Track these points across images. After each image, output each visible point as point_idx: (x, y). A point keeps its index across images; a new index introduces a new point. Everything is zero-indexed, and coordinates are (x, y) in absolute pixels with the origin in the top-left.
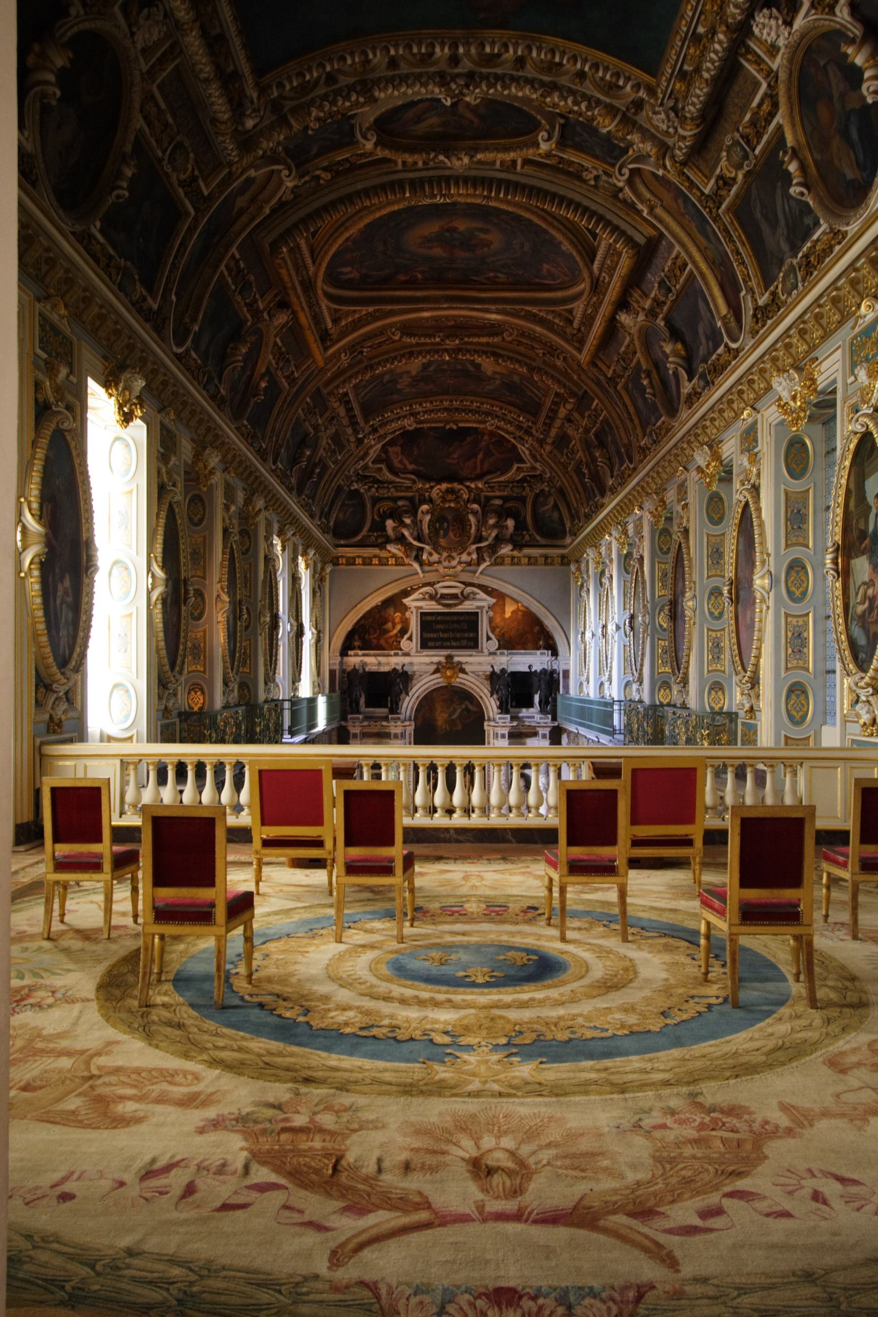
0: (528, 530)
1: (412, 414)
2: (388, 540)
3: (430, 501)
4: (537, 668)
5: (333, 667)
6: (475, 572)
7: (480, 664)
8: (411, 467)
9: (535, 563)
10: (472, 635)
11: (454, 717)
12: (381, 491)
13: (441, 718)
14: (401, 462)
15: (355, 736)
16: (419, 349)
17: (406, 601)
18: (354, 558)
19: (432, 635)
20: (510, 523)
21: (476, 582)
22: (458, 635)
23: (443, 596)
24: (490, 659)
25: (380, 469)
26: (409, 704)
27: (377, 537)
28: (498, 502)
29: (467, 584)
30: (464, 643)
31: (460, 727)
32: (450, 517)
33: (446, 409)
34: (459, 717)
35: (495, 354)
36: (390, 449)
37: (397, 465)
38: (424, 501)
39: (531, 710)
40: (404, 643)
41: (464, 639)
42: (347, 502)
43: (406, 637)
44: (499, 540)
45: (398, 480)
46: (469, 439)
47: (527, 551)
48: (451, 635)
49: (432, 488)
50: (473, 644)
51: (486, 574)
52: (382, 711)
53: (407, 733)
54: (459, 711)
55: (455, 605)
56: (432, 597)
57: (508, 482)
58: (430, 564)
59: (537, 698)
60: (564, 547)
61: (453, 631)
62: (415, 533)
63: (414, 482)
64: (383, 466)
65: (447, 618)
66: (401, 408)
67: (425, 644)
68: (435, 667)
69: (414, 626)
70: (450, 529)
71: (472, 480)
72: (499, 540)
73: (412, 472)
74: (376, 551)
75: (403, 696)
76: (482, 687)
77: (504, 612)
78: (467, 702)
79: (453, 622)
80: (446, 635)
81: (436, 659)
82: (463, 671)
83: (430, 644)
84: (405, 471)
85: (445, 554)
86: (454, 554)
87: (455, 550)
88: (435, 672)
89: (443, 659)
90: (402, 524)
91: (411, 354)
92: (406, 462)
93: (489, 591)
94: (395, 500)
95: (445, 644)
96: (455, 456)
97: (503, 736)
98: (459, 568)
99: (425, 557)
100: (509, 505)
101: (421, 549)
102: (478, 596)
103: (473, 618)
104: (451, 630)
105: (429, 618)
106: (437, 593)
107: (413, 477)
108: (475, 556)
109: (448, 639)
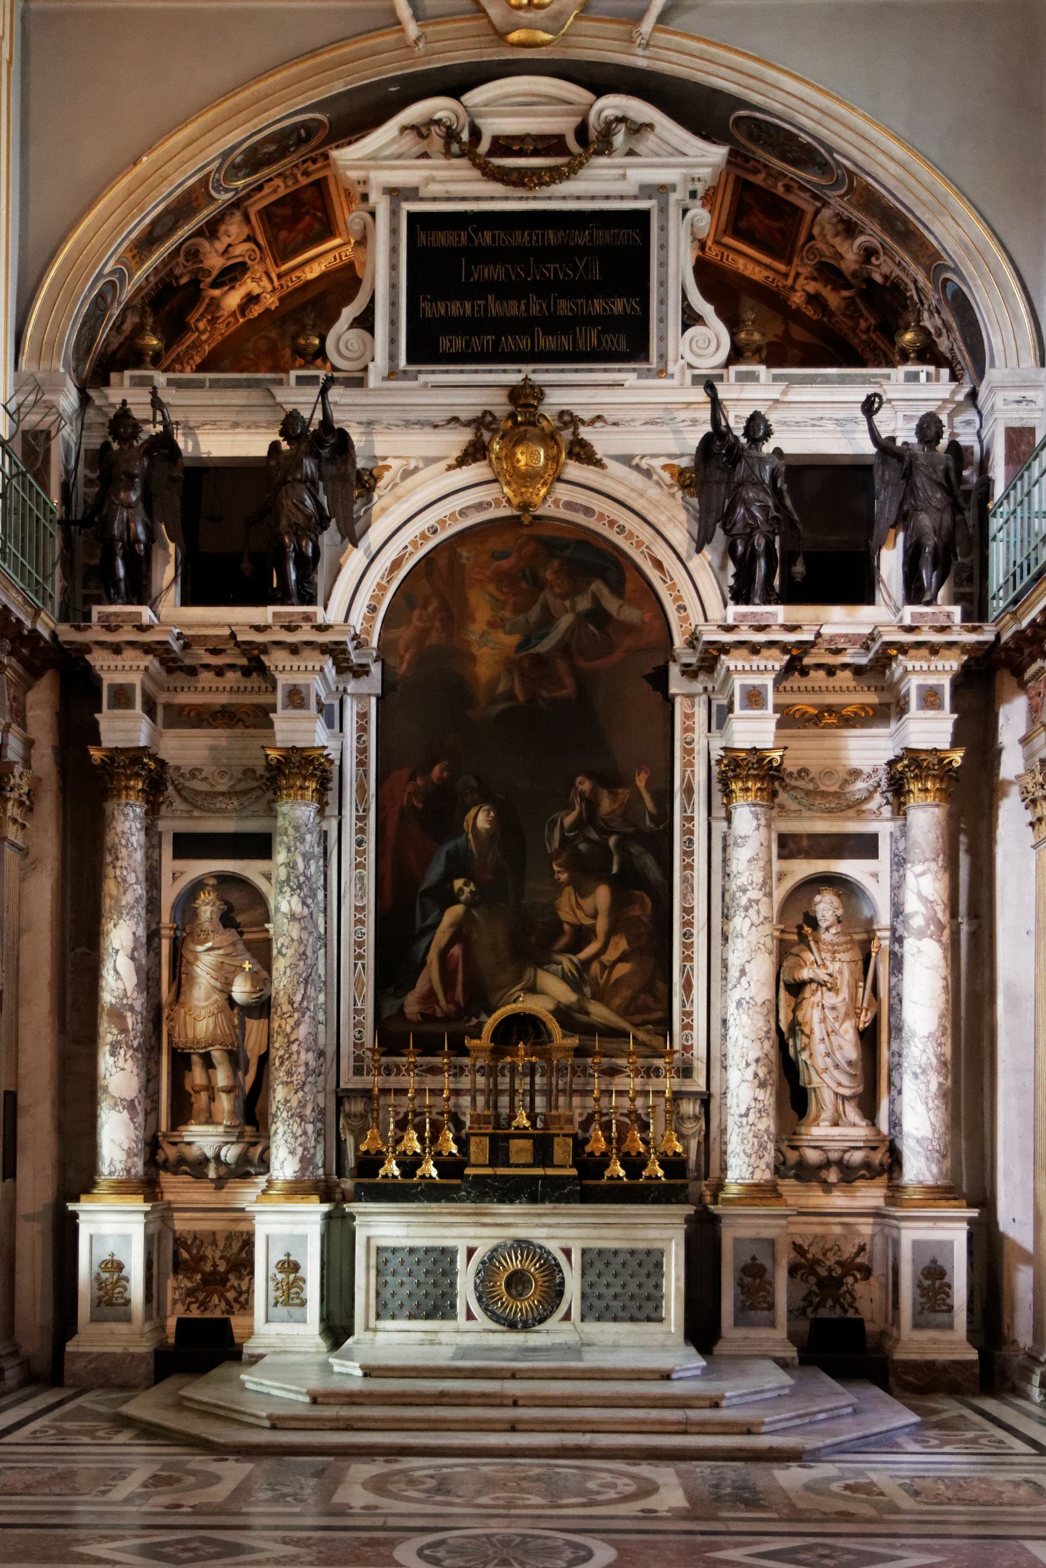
4: (899, 426)
10: (619, 306)
11: (544, 646)
13: (489, 646)
17: (350, 157)
19: (455, 309)
22: (564, 307)
23: (504, 145)
29: (600, 79)
39: (864, 612)
40: (341, 338)
43: (349, 313)
54: (565, 621)
55: (556, 175)
56: (461, 143)
59: (891, 562)
61: (544, 289)
65: (521, 238)
67: (426, 347)
69: (385, 272)
78: (597, 586)
79: (545, 254)
80: (513, 309)
82: (582, 452)
83: (445, 344)
88: (462, 461)
89: (498, 403)
93: (698, 108)
95: (509, 343)
102: (649, 143)
105: (442, 238)
106: (476, 134)
109: (523, 325)
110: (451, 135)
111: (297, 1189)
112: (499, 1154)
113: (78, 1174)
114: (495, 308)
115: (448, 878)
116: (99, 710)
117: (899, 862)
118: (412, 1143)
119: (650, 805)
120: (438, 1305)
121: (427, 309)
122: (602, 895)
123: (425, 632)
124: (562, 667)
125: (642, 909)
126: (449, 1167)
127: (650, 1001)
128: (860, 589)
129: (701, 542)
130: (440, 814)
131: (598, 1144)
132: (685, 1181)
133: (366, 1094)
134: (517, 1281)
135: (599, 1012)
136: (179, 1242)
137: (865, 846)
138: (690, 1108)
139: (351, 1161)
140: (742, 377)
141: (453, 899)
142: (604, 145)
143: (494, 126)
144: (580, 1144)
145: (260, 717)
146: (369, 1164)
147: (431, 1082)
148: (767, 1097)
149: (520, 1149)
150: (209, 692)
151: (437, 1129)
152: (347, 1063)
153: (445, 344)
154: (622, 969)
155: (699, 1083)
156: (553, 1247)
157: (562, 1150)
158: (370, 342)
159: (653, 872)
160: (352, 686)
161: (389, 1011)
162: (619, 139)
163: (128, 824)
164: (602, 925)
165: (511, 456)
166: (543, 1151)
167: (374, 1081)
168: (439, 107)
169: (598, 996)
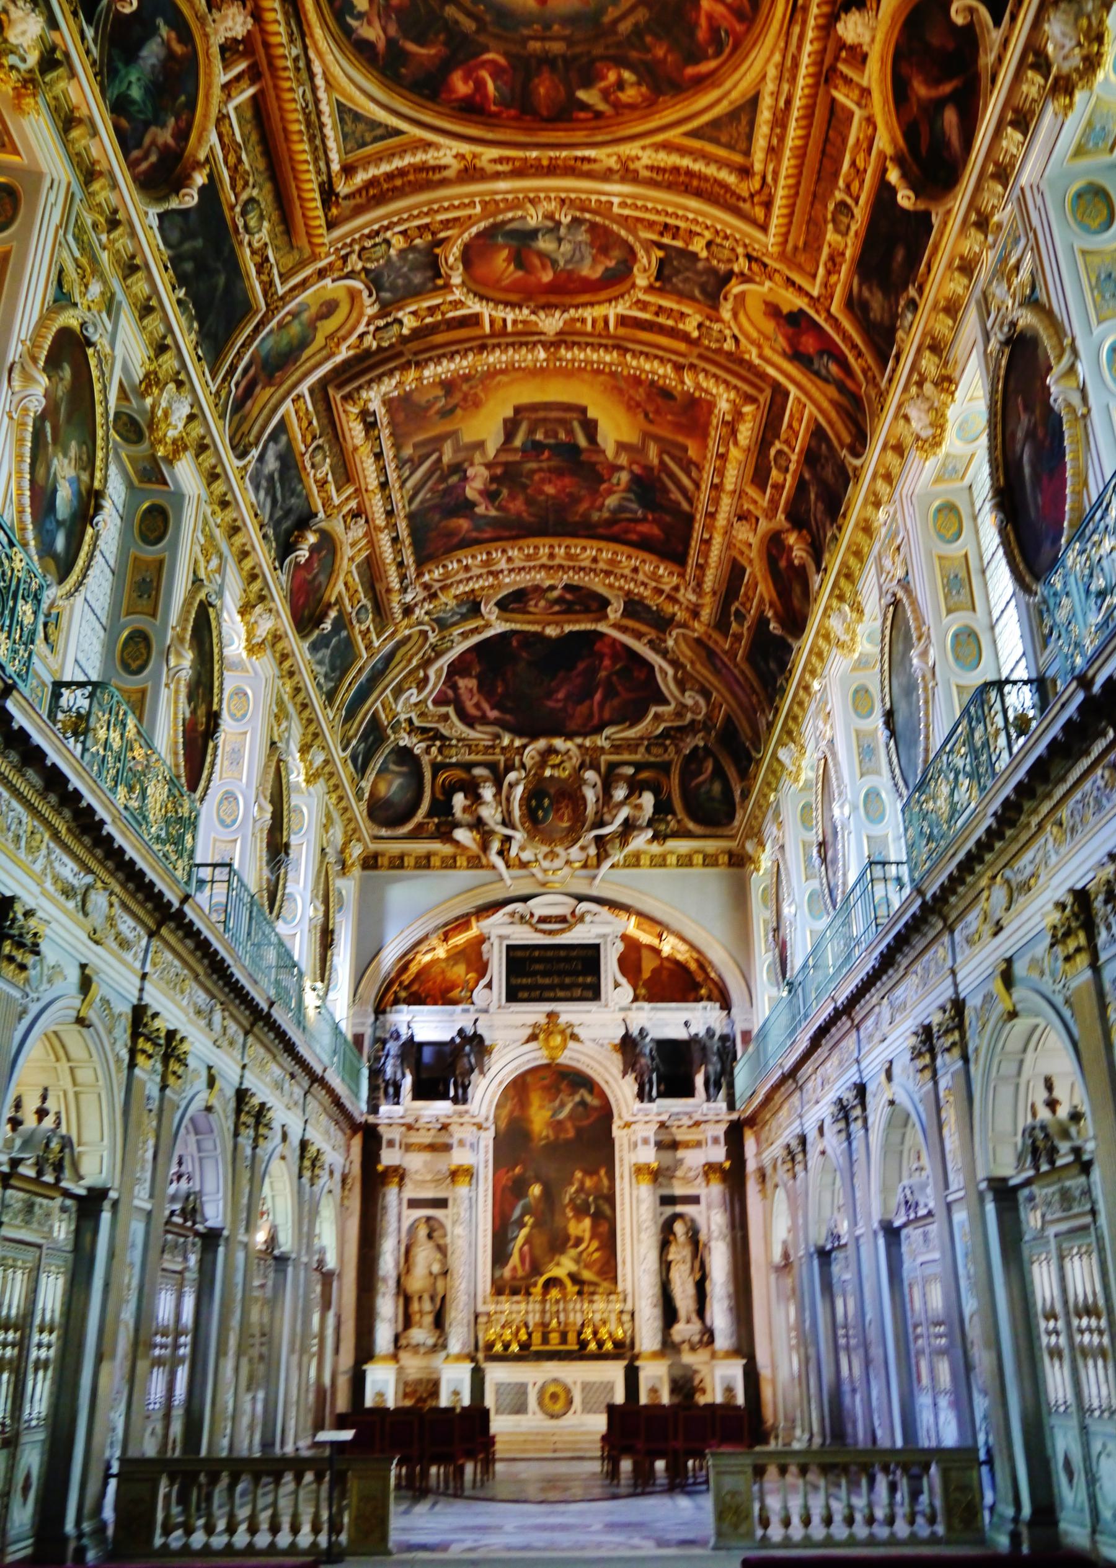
0: (674, 814)
1: (491, 573)
2: (457, 825)
3: (523, 766)
5: (360, 1030)
6: (594, 877)
7: (603, 1025)
8: (493, 714)
9: (690, 864)
12: (446, 752)
13: (540, 1117)
14: (477, 706)
15: (391, 1144)
16: (495, 341)
18: (401, 858)
19: (524, 981)
20: (648, 800)
21: (594, 892)
22: (567, 980)
23: (543, 920)
24: (622, 1015)
25: (445, 717)
26: (486, 1091)
27: (438, 826)
28: (630, 771)
29: (581, 898)
30: (578, 992)
31: (571, 1134)
32: (552, 791)
33: (543, 566)
34: (571, 1117)
35: (617, 347)
36: (463, 683)
37: (473, 712)
38: (510, 768)
41: (578, 985)
42: (393, 767)
43: (483, 982)
44: (629, 827)
45: (472, 734)
46: (581, 666)
47: (671, 844)
48: (556, 980)
49: (524, 747)
50: (593, 993)
51: (608, 880)
52: (441, 1108)
53: (482, 1144)
55: (562, 931)
57: (642, 738)
58: (524, 865)
60: (732, 837)
61: (560, 973)
62: (499, 817)
63: (498, 736)
64: (450, 710)
65: (550, 954)
66: (474, 557)
67: (513, 995)
68: (529, 1031)
70: (551, 808)
71: (585, 735)
72: (629, 827)
73: (496, 722)
74: (436, 846)
75: (474, 1076)
76: (608, 1064)
77: (639, 970)
79: (559, 960)
80: (547, 981)
81: (531, 1019)
82: (574, 1037)
83: (521, 995)
84: (484, 720)
85: (546, 849)
86: (559, 850)
87: (562, 841)
88: (527, 1041)
89: (542, 1020)
90: (476, 798)
91: (482, 348)
92: (486, 706)
94: (468, 766)
95: (546, 994)
96: (561, 695)
97: (646, 1141)
98: (567, 870)
99: (514, 852)
100: (644, 775)
101: (508, 839)
103: (590, 952)
104: (553, 972)
105: (519, 954)
107: (496, 729)
108: (592, 851)
109: (551, 987)
110: (522, 917)
111: (459, 1358)
112: (545, 1340)
113: (365, 1352)
114: (540, 980)
115: (522, 1216)
116: (380, 1148)
117: (709, 1207)
118: (508, 1335)
119: (606, 1182)
120: (520, 1408)
121: (514, 981)
122: (587, 1222)
123: (512, 1112)
124: (569, 1125)
125: (604, 1228)
126: (525, 1346)
127: (608, 1268)
128: (689, 1092)
129: (625, 1074)
130: (518, 1188)
131: (588, 1333)
132: (624, 1350)
133: (488, 1314)
134: (554, 1397)
135: (587, 1275)
136: (406, 1384)
137: (695, 1200)
138: (626, 1317)
139: (481, 1344)
140: (639, 1009)
141: (522, 1225)
142: (581, 919)
143: (539, 912)
144: (580, 1333)
145: (447, 1148)
146: (490, 1346)
147: (515, 1307)
148: (657, 1312)
149: (554, 1337)
150: (426, 1138)
151: (518, 1330)
152: (480, 1299)
153: (521, 995)
154: (596, 1255)
155: (629, 1307)
156: (569, 1381)
157: (572, 1337)
158: (491, 993)
159: (608, 1212)
160: (483, 1134)
161: (498, 1274)
162: (588, 918)
163: (391, 1195)
164: (587, 1235)
165: (547, 1040)
166: (564, 1339)
167: (492, 1308)
168: (518, 907)
169: (587, 1266)
